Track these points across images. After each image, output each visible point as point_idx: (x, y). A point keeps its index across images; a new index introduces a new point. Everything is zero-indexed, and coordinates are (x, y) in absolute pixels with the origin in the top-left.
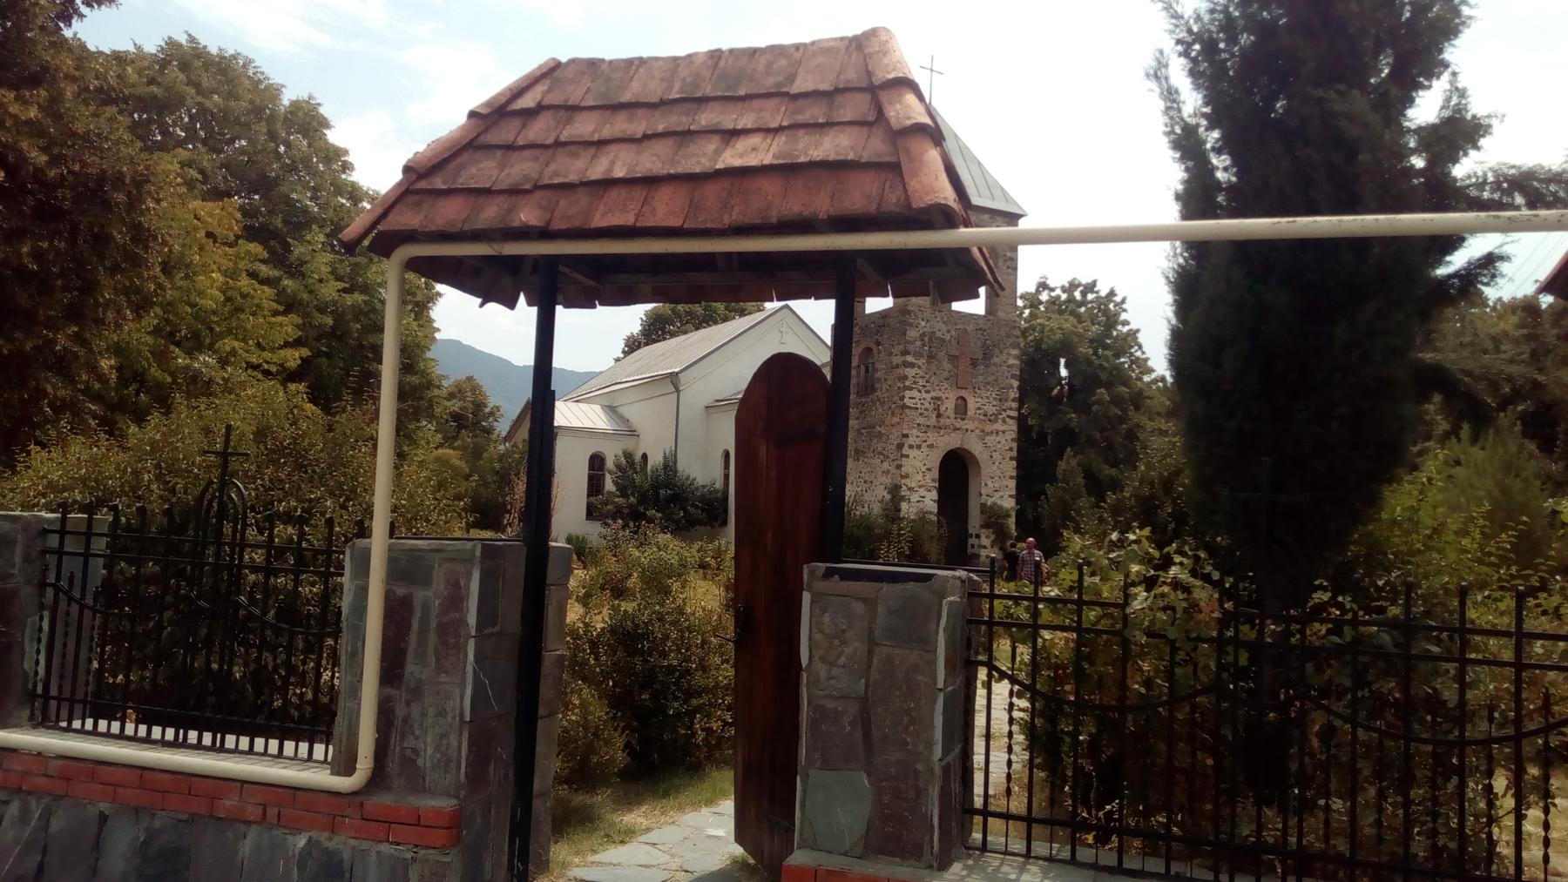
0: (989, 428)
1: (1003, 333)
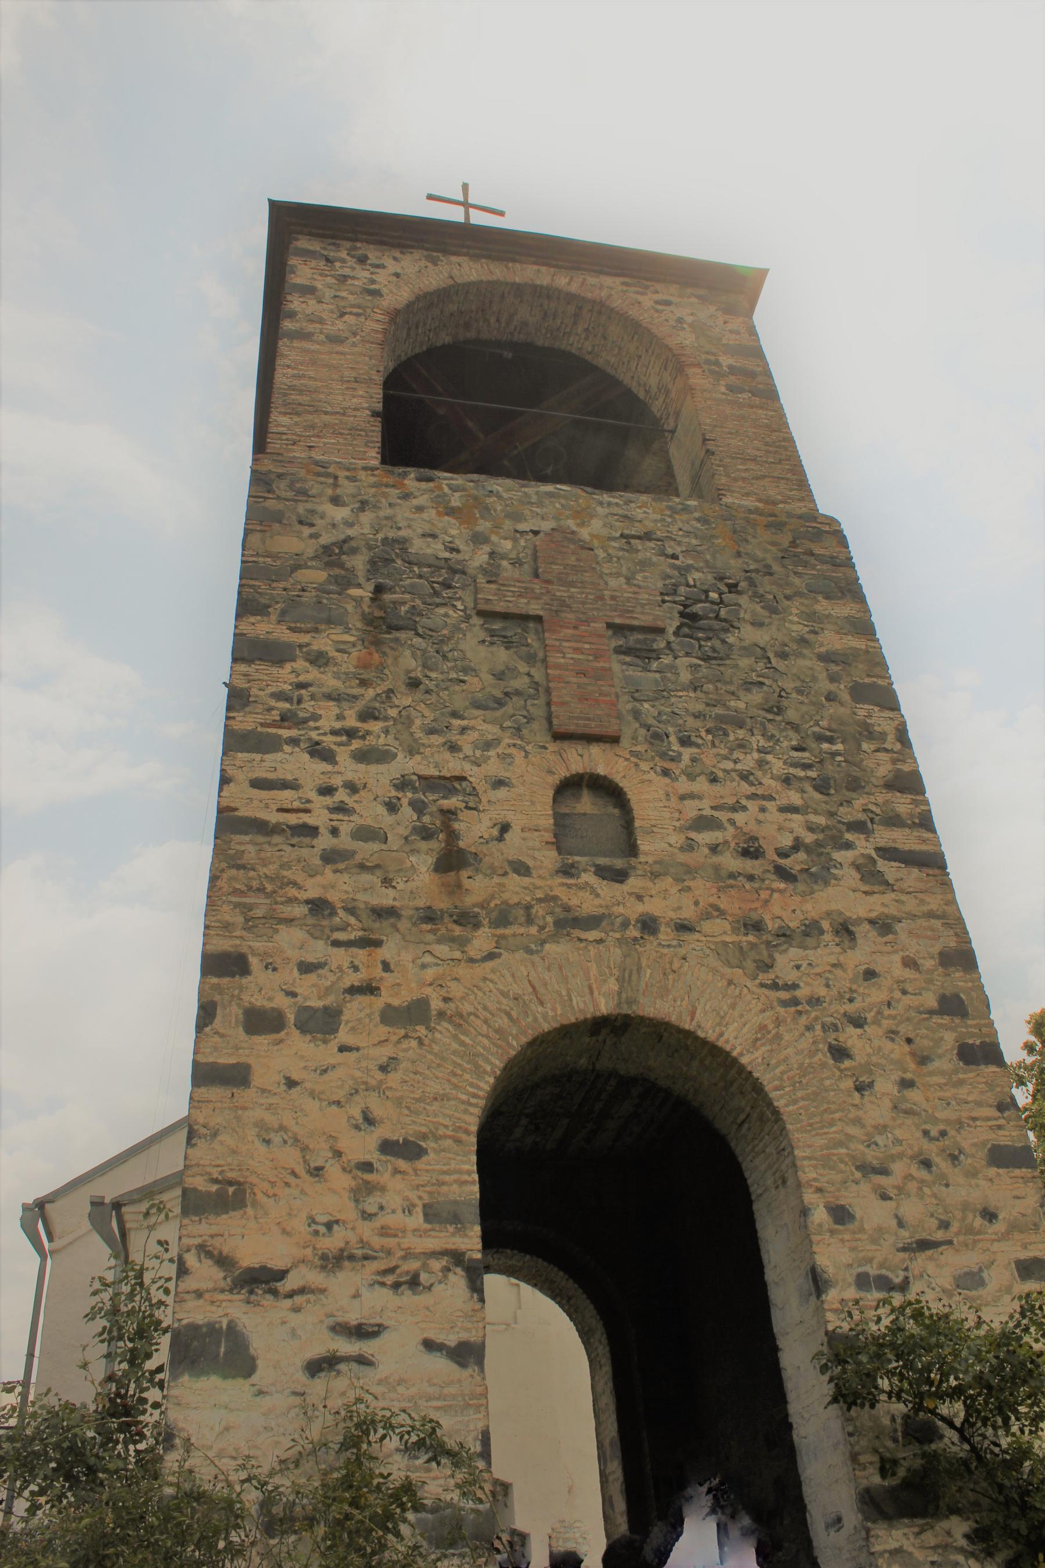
0: (785, 908)
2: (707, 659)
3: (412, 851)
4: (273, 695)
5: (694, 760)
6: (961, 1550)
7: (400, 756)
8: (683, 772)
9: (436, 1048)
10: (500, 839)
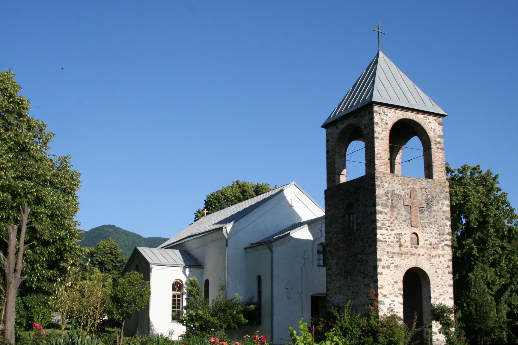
0: (434, 253)
1: (438, 190)
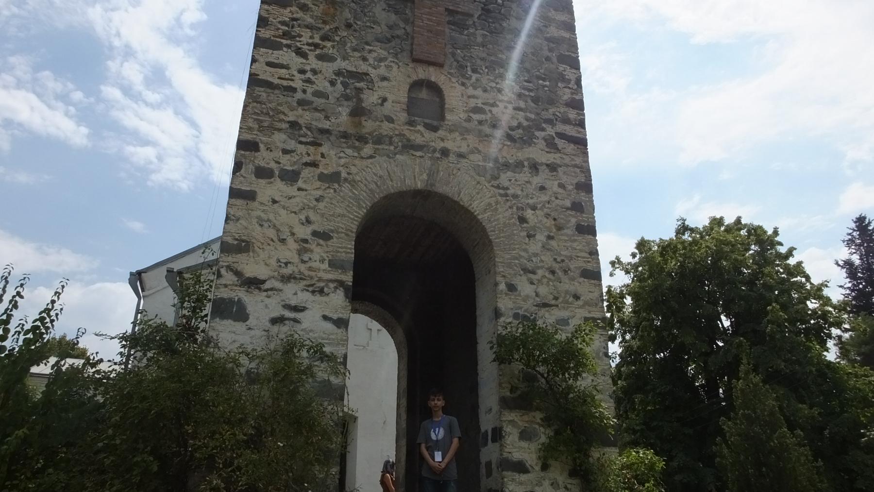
2: (491, 32)
3: (340, 105)
4: (280, 22)
5: (477, 80)
6: (538, 424)
7: (339, 60)
8: (471, 85)
9: (342, 194)
10: (382, 105)
